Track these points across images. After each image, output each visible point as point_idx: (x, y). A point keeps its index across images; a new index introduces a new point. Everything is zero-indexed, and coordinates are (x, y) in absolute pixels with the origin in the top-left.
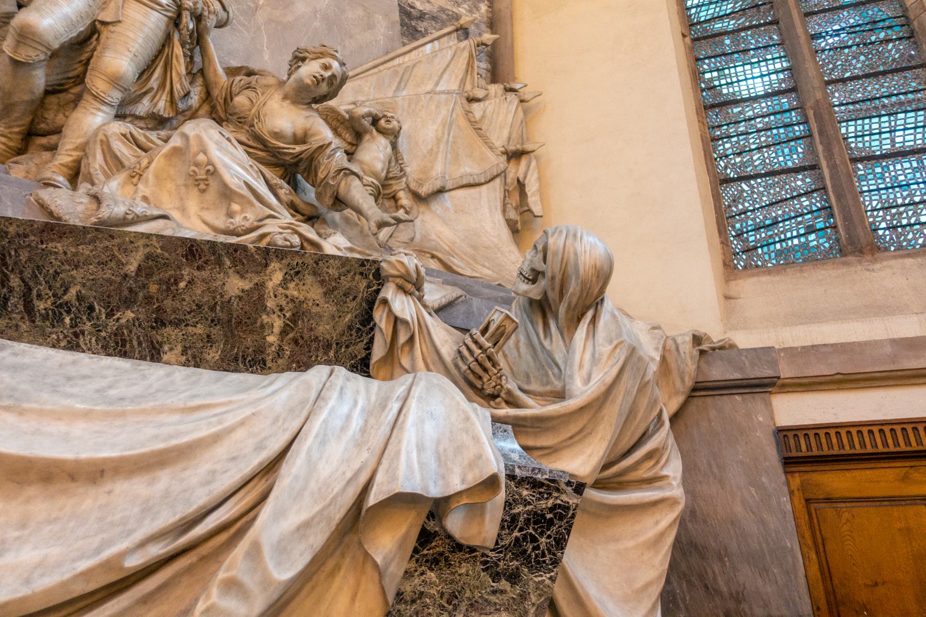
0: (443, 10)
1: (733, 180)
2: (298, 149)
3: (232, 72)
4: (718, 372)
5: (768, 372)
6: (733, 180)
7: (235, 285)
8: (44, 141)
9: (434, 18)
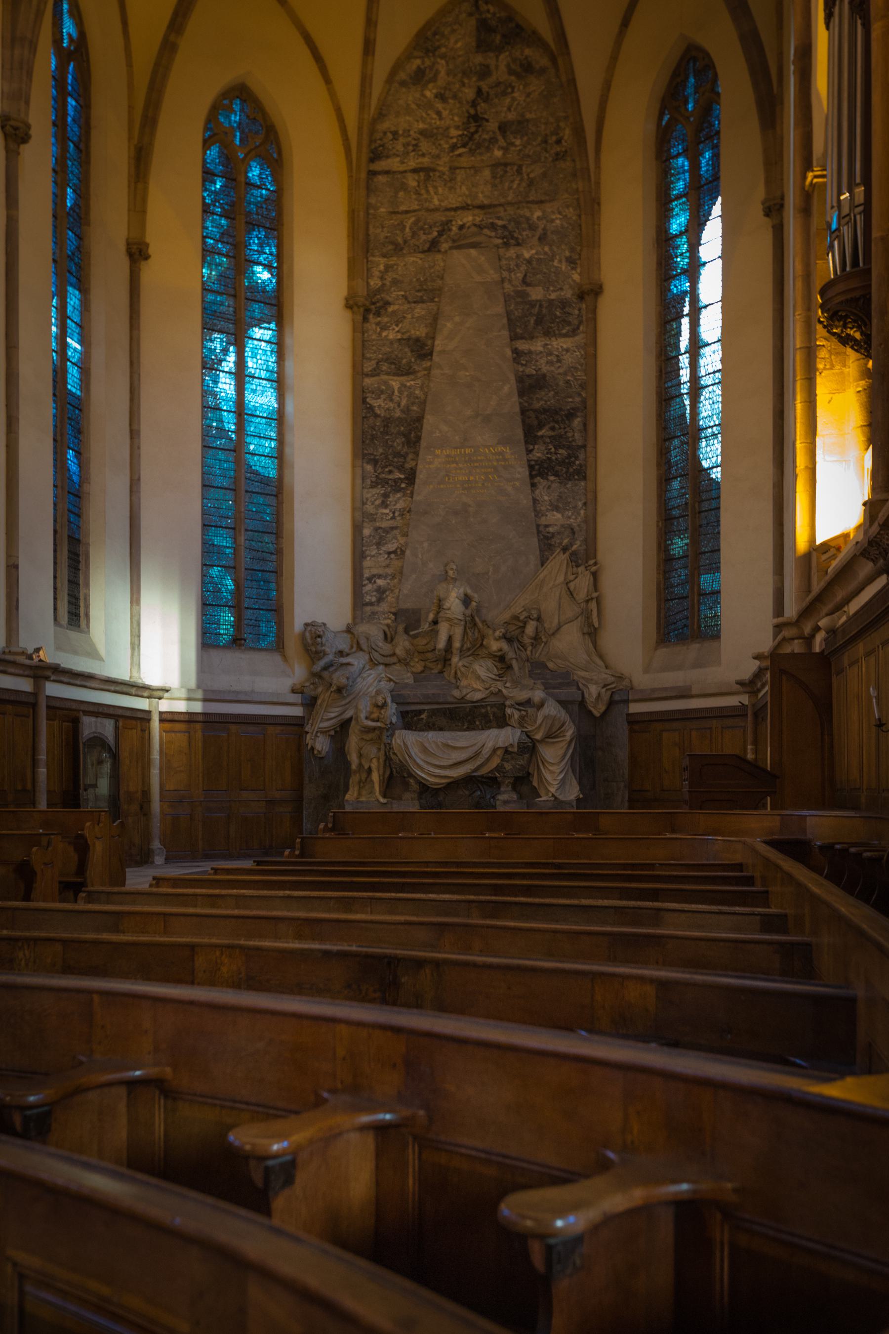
0: (562, 526)
1: (668, 600)
2: (499, 653)
3: (484, 622)
4: (617, 697)
5: (626, 698)
6: (668, 600)
7: (483, 711)
8: (448, 663)
9: (559, 533)
